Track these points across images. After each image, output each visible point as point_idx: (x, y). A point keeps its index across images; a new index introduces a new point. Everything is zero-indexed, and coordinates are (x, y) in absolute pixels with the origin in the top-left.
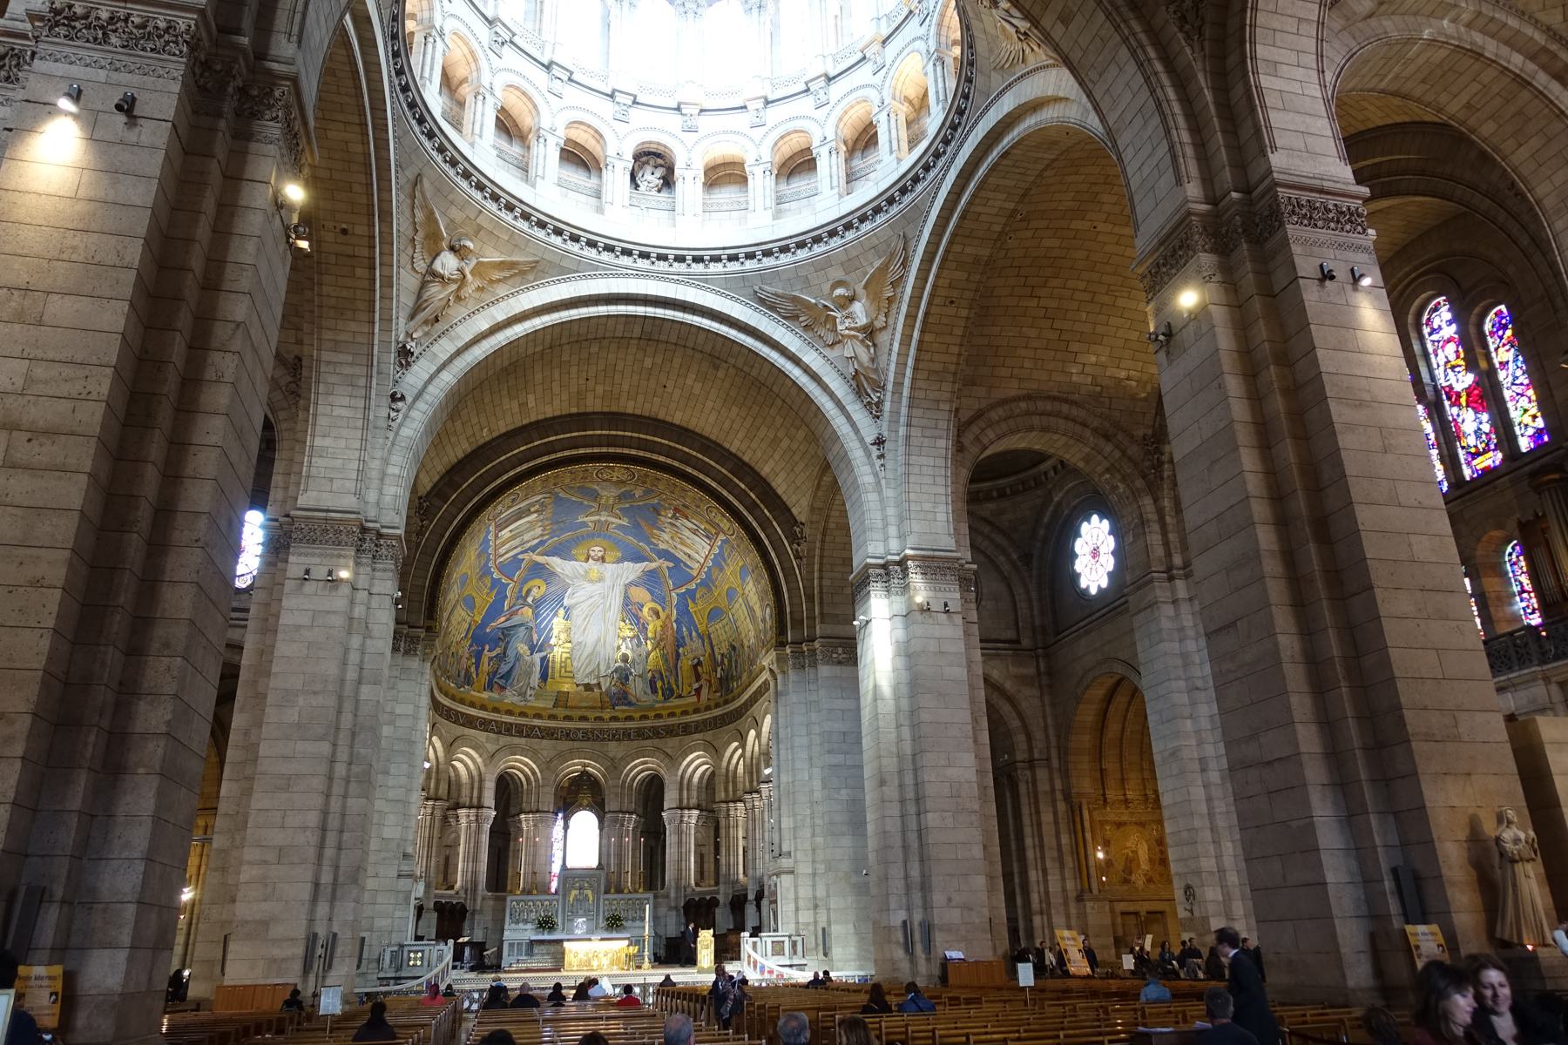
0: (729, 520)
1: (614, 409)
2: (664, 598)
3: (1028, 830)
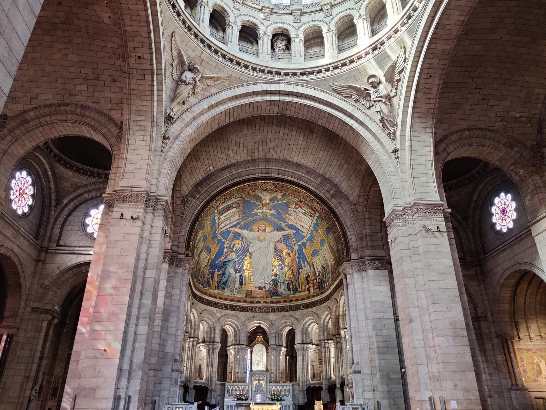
0: (320, 205)
1: (267, 157)
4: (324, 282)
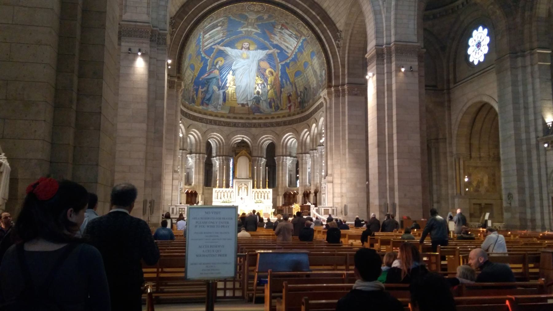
0: (307, 30)
3: (434, 169)
4: (305, 102)
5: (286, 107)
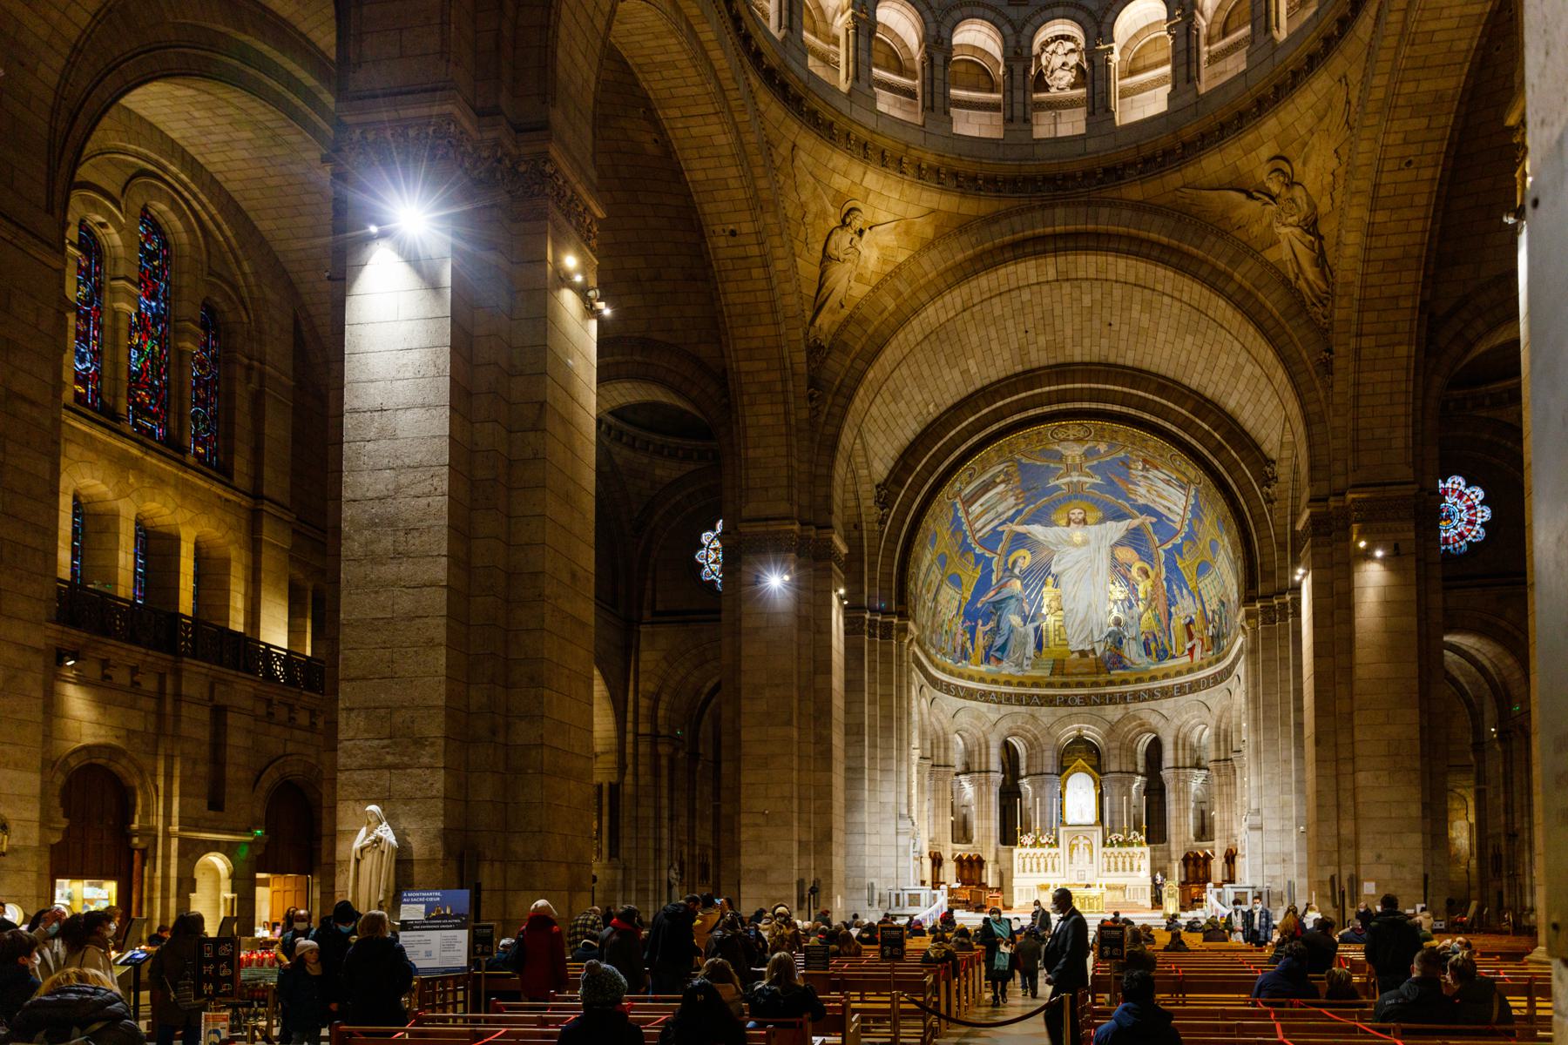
2: (1151, 556)
4: (1224, 636)
5: (1181, 649)
